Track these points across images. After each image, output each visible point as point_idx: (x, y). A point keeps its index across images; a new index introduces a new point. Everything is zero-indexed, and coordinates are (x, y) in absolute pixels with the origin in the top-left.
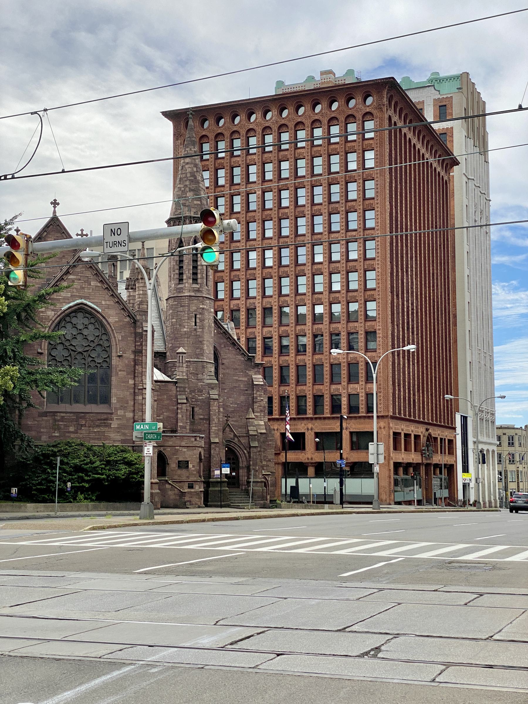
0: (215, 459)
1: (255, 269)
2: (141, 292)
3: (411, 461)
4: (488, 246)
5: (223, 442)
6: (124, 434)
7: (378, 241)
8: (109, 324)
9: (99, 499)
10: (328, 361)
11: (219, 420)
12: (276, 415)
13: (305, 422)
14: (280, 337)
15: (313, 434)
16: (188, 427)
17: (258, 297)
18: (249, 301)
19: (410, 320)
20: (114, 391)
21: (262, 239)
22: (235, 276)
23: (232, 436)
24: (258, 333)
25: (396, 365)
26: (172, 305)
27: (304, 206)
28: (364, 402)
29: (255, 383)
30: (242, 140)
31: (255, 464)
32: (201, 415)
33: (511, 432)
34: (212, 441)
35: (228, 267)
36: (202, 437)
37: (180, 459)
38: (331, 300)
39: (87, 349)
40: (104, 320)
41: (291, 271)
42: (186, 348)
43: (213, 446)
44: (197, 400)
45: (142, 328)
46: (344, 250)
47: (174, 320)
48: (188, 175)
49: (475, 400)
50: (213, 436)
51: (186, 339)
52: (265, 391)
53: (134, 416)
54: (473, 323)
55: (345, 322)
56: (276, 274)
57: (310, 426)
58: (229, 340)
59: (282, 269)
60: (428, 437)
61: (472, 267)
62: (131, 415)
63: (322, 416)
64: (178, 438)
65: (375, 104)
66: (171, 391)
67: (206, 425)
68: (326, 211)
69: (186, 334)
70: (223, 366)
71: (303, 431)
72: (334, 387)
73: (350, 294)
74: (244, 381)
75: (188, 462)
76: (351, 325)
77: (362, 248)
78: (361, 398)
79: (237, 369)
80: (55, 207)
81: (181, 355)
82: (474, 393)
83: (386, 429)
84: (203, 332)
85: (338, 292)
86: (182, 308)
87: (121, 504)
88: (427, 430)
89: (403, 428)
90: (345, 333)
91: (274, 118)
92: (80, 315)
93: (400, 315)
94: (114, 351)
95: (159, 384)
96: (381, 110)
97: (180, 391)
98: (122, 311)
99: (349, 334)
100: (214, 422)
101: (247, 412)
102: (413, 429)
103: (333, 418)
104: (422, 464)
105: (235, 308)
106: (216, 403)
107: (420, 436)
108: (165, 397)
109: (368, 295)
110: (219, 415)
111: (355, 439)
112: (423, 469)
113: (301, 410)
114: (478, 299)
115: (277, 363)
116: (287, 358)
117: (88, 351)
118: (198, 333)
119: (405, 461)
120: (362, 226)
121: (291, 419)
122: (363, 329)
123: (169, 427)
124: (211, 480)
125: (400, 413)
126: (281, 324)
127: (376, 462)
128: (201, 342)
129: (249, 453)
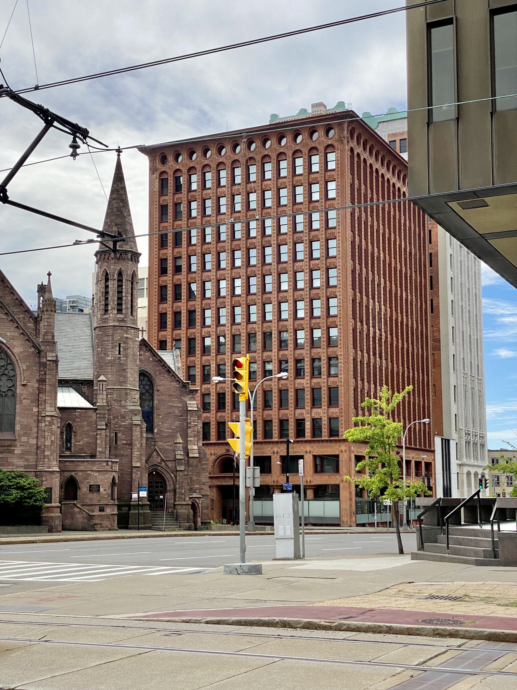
1: (224, 297)
4: (477, 272)
5: (146, 467)
6: (27, 460)
7: (340, 269)
10: (293, 386)
15: (278, 457)
17: (227, 325)
18: (250, 326)
19: (377, 345)
20: (17, 418)
21: (232, 269)
23: (159, 461)
26: (98, 335)
27: (270, 236)
28: (326, 426)
29: (189, 409)
31: (181, 488)
32: (124, 440)
33: (507, 455)
34: (134, 466)
35: (244, 292)
36: (117, 462)
37: (92, 484)
38: (296, 326)
40: (8, 351)
41: (258, 299)
42: (110, 376)
43: (134, 470)
44: (120, 426)
46: (307, 278)
49: (460, 423)
50: (136, 460)
51: (110, 367)
53: (38, 442)
54: (457, 347)
55: (308, 348)
56: (245, 302)
57: (276, 449)
58: (164, 367)
61: (456, 292)
62: (34, 441)
64: (90, 462)
65: (336, 136)
66: (91, 417)
67: (129, 450)
69: (109, 362)
71: (269, 455)
72: (298, 411)
73: (313, 321)
74: (179, 407)
75: (99, 486)
76: (314, 350)
77: (324, 276)
79: (172, 395)
81: (101, 383)
82: (460, 416)
83: (348, 452)
84: (126, 360)
86: (106, 338)
87: (13, 527)
91: (242, 152)
94: (18, 380)
95: (79, 411)
97: (99, 418)
99: (313, 360)
100: (135, 447)
103: (281, 442)
106: (138, 429)
108: (86, 423)
110: (142, 440)
114: (464, 323)
115: (276, 387)
118: (122, 362)
123: (89, 452)
128: (124, 370)
129: (176, 476)
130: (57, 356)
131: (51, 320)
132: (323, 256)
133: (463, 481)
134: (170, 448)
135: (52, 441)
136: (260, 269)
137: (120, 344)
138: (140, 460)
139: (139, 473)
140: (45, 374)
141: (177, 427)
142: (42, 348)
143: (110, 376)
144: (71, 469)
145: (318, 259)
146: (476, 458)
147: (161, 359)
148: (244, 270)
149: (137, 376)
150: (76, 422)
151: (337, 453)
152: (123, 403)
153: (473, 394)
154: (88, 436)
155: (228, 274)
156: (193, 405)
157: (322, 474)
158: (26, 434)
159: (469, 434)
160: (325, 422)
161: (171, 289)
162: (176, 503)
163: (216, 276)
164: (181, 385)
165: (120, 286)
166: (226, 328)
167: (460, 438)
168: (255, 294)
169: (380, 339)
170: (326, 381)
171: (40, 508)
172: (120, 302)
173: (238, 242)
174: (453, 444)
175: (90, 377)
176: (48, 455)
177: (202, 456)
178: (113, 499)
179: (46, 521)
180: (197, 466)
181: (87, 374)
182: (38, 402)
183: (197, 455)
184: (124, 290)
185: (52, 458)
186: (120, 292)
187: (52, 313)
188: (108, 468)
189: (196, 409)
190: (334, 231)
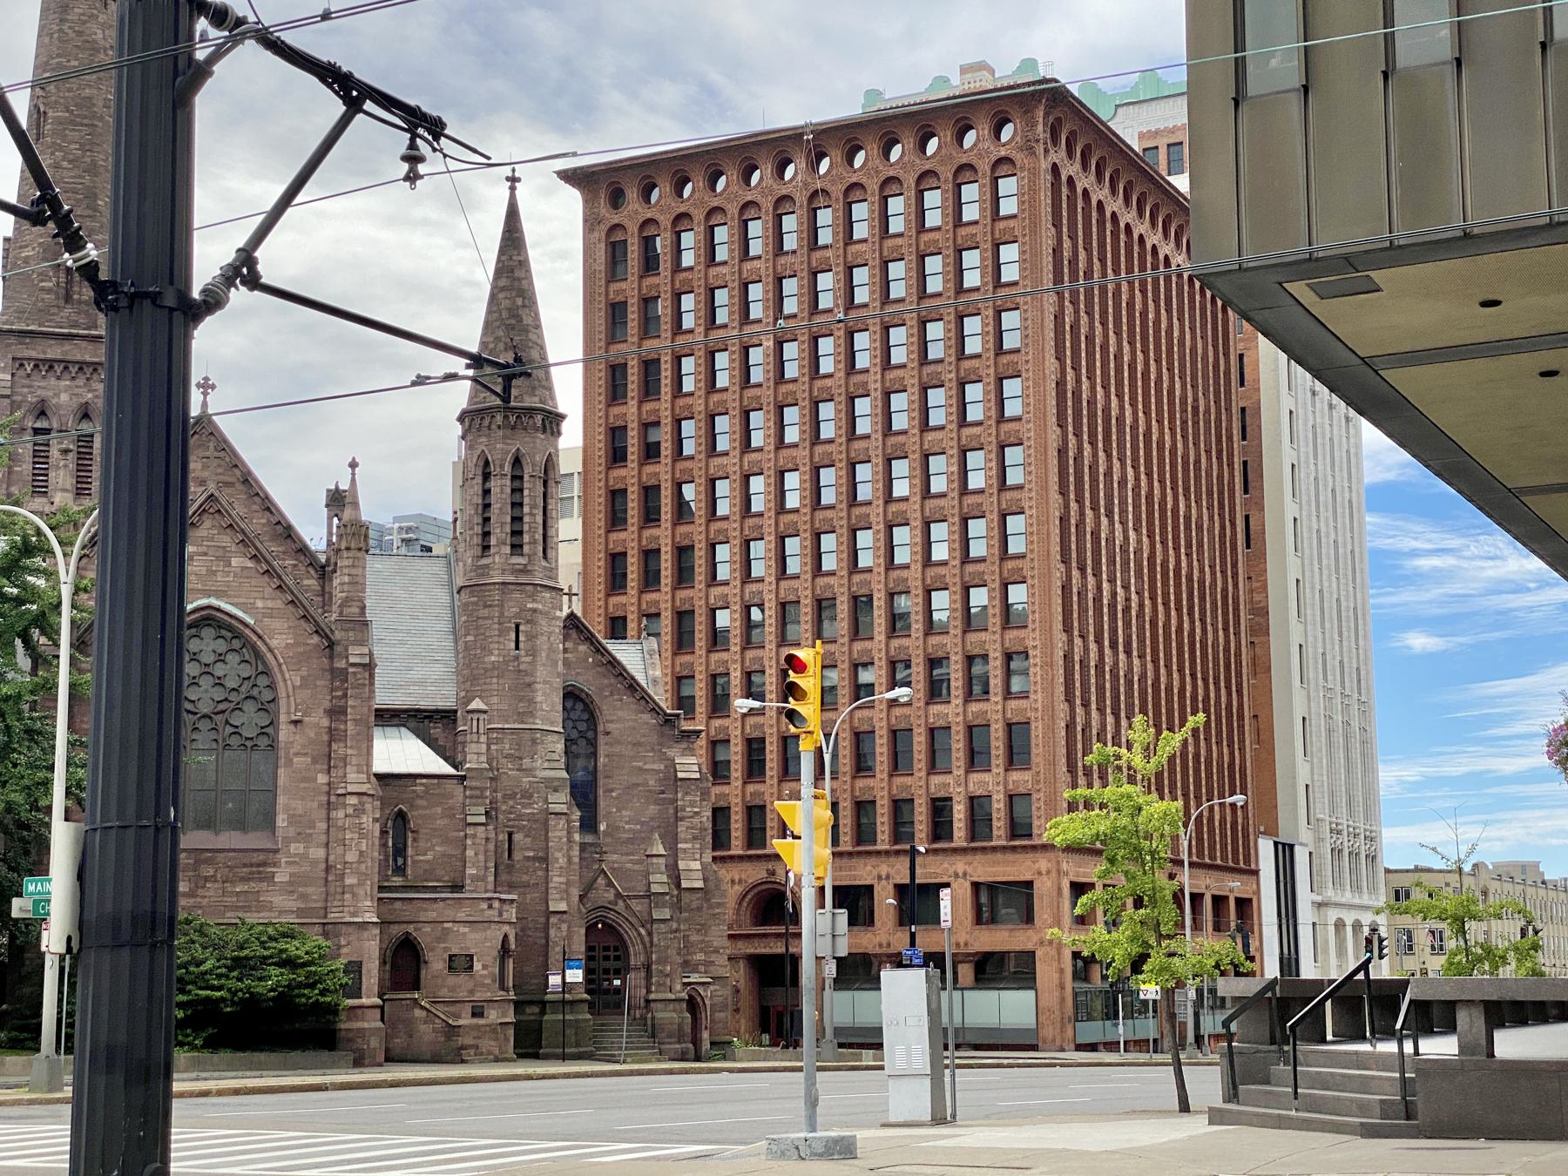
1: (761, 515)
4: (1352, 451)
6: (303, 897)
8: (271, 650)
9: (212, 1044)
12: (737, 848)
13: (873, 860)
15: (891, 888)
17: (767, 579)
18: (821, 581)
19: (1120, 624)
20: (281, 800)
21: (777, 449)
23: (611, 895)
26: (466, 604)
27: (866, 371)
29: (680, 775)
30: (732, 228)
31: (663, 961)
32: (528, 849)
36: (512, 901)
37: (455, 951)
38: (929, 581)
39: (221, 707)
40: (259, 643)
41: (840, 518)
43: (553, 920)
44: (520, 817)
46: (955, 469)
47: (470, 638)
48: (505, 314)
49: (1318, 805)
55: (959, 631)
56: (808, 526)
57: (884, 869)
61: (1304, 498)
62: (321, 853)
65: (1018, 139)
67: (540, 873)
68: (916, 381)
71: (868, 882)
72: (936, 780)
75: (471, 956)
76: (972, 637)
79: (637, 744)
80: (205, 394)
81: (475, 716)
83: (1054, 874)
90: (958, 658)
91: (799, 177)
92: (208, 633)
94: (283, 710)
96: (1031, 151)
98: (302, 622)
99: (970, 660)
101: (648, 840)
103: (898, 853)
108: (439, 810)
110: (570, 849)
114: (1325, 572)
115: (884, 723)
117: (223, 712)
118: (522, 667)
128: (529, 685)
129: (650, 934)
130: (371, 655)
131: (358, 571)
133: (1326, 941)
134: (636, 867)
135: (361, 852)
136: (844, 448)
138: (566, 894)
139: (564, 927)
140: (345, 695)
141: (652, 819)
142: (338, 635)
143: (495, 700)
145: (979, 424)
146: (1356, 888)
148: (807, 452)
149: (557, 699)
150: (418, 808)
151: (1028, 877)
152: (526, 762)
153: (1347, 737)
154: (446, 841)
155: (768, 460)
156: (690, 765)
158: (301, 837)
160: (998, 805)
162: (652, 996)
164: (661, 719)
165: (516, 490)
167: (1319, 840)
169: (1127, 610)
170: (1000, 707)
171: (333, 1010)
172: (517, 528)
173: (791, 387)
174: (1301, 856)
176: (351, 886)
177: (712, 885)
178: (503, 987)
179: (350, 1040)
180: (699, 909)
181: (442, 696)
182: (328, 761)
183: (700, 884)
184: (526, 501)
186: (516, 505)
187: (359, 554)
188: (492, 914)
189: (697, 776)
190: (1014, 357)
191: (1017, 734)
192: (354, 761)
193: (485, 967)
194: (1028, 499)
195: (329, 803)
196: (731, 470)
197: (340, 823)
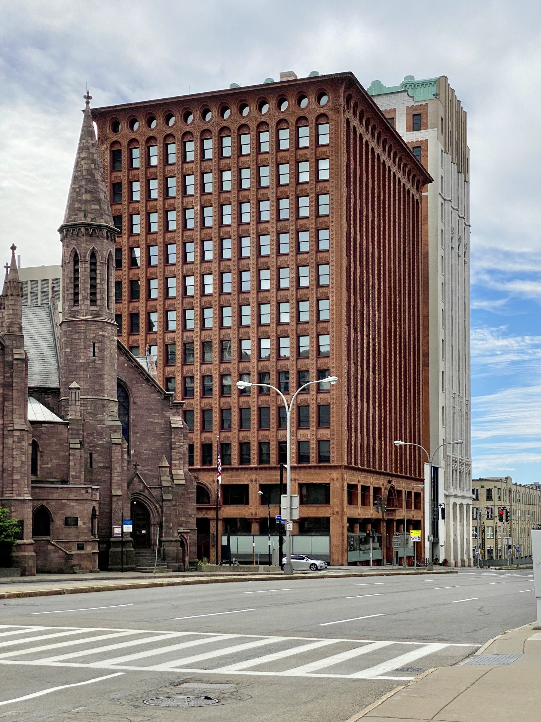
0: (117, 514)
2: (11, 312)
3: (370, 517)
5: (128, 495)
7: (333, 265)
10: (275, 403)
11: (122, 469)
14: (222, 377)
15: (257, 486)
16: (83, 477)
17: (195, 330)
19: (371, 357)
22: (170, 305)
23: (141, 487)
24: (196, 369)
25: (353, 408)
26: (66, 331)
27: (248, 224)
28: (315, 450)
29: (173, 426)
34: (114, 494)
36: (97, 489)
41: (234, 299)
42: (82, 383)
45: (12, 355)
46: (294, 275)
47: (68, 350)
50: (116, 487)
51: (82, 372)
52: (185, 437)
53: (3, 463)
56: (217, 303)
57: (254, 477)
58: (142, 375)
59: (223, 297)
60: (390, 491)
63: (267, 466)
64: (65, 489)
66: (61, 434)
68: (274, 230)
69: (82, 366)
70: (135, 406)
71: (246, 483)
74: (161, 424)
75: (77, 518)
77: (314, 274)
78: (311, 446)
79: (152, 410)
81: (74, 391)
83: (340, 480)
85: (287, 324)
86: (77, 335)
88: (389, 482)
89: (360, 479)
93: (359, 351)
95: (46, 425)
97: (72, 434)
100: (116, 471)
101: (160, 460)
102: (372, 481)
104: (383, 520)
105: (171, 342)
106: (118, 448)
107: (380, 489)
108: (54, 441)
109: (320, 328)
110: (123, 462)
111: (304, 492)
112: (383, 527)
113: (244, 459)
114: (454, 337)
116: (228, 400)
118: (97, 366)
119: (362, 517)
120: (314, 247)
121: (223, 470)
122: (314, 366)
123: (59, 477)
124: (112, 539)
125: (356, 463)
126: (222, 361)
127: (289, 517)
129: (162, 507)
130: (26, 354)
131: (18, 308)
132: (312, 250)
134: (149, 473)
135: (22, 462)
136: (236, 263)
137: (94, 344)
138: (120, 487)
139: (120, 503)
140: (12, 376)
141: (158, 448)
142: (7, 343)
144: (42, 498)
145: (307, 253)
146: (462, 488)
147: (139, 364)
148: (217, 265)
150: (43, 439)
151: (327, 481)
152: (99, 416)
153: (460, 417)
155: (196, 268)
157: (309, 505)
159: (456, 462)
160: (313, 445)
161: (126, 285)
162: (163, 539)
163: (182, 271)
166: (194, 334)
167: (448, 465)
168: (230, 294)
169: (374, 350)
170: (314, 397)
172: (93, 291)
173: (208, 231)
175: (55, 385)
176: (16, 479)
178: (93, 535)
179: (18, 562)
180: (183, 495)
181: (52, 382)
183: (183, 482)
184: (98, 276)
185: (22, 483)
186: (93, 279)
187: (18, 298)
189: (182, 426)
190: (325, 219)
191: (323, 410)
192: (17, 412)
193: (84, 523)
194: (332, 292)
195: (3, 434)
196: (177, 273)
197: (10, 446)
